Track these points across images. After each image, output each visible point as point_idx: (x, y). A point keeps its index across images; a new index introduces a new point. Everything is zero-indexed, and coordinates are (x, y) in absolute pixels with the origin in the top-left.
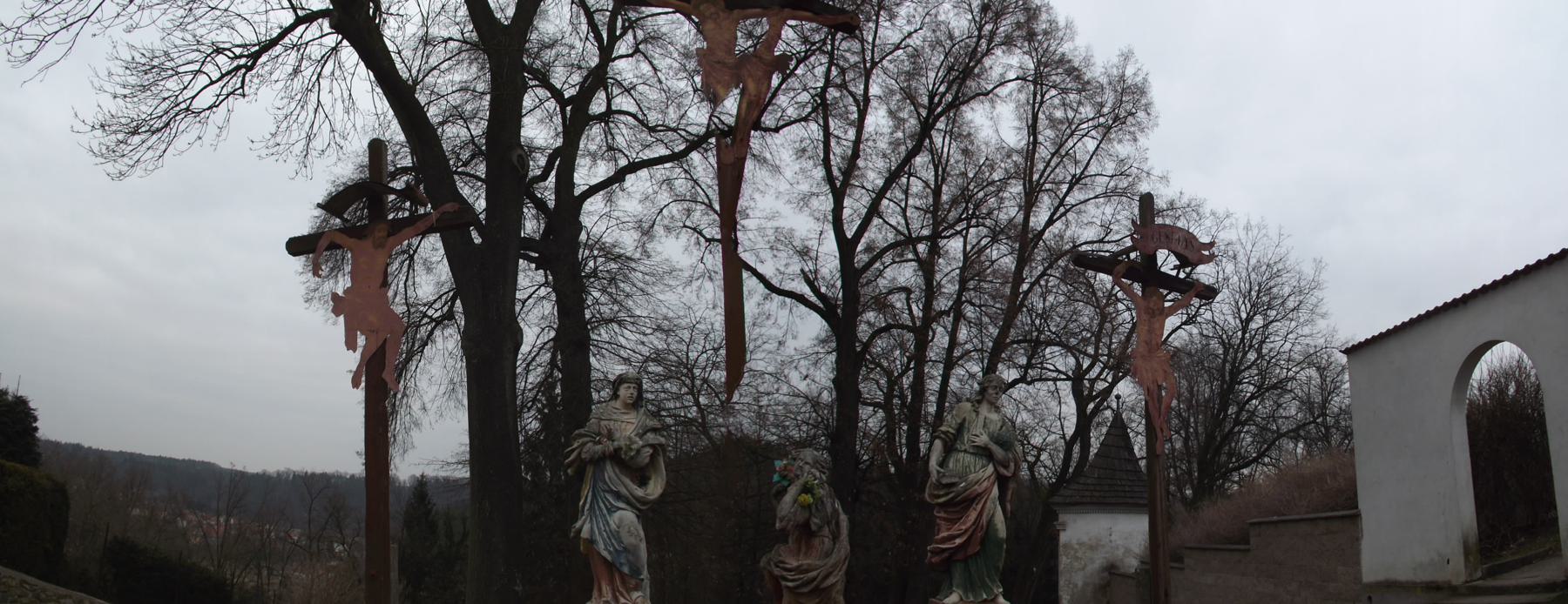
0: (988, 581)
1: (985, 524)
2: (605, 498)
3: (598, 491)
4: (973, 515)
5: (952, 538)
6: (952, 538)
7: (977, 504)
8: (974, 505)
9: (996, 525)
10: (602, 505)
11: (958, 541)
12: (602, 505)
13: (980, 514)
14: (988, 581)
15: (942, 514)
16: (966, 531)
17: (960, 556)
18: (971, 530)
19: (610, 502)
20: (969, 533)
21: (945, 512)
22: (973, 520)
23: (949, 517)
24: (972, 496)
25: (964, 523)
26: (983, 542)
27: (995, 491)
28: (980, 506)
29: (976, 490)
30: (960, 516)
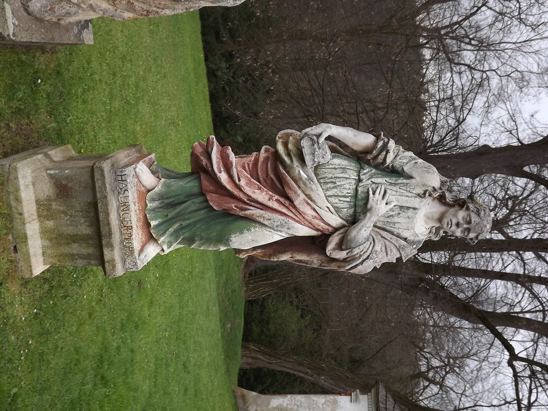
0: (176, 226)
1: (248, 212)
4: (262, 196)
5: (228, 168)
6: (228, 168)
7: (277, 201)
8: (277, 197)
9: (248, 230)
11: (223, 177)
14: (176, 226)
15: (263, 154)
16: (239, 187)
17: (206, 183)
18: (241, 195)
20: (236, 192)
21: (267, 159)
22: (254, 196)
23: (260, 164)
24: (288, 191)
25: (249, 184)
26: (227, 214)
27: (303, 231)
28: (276, 205)
29: (298, 196)
30: (261, 179)
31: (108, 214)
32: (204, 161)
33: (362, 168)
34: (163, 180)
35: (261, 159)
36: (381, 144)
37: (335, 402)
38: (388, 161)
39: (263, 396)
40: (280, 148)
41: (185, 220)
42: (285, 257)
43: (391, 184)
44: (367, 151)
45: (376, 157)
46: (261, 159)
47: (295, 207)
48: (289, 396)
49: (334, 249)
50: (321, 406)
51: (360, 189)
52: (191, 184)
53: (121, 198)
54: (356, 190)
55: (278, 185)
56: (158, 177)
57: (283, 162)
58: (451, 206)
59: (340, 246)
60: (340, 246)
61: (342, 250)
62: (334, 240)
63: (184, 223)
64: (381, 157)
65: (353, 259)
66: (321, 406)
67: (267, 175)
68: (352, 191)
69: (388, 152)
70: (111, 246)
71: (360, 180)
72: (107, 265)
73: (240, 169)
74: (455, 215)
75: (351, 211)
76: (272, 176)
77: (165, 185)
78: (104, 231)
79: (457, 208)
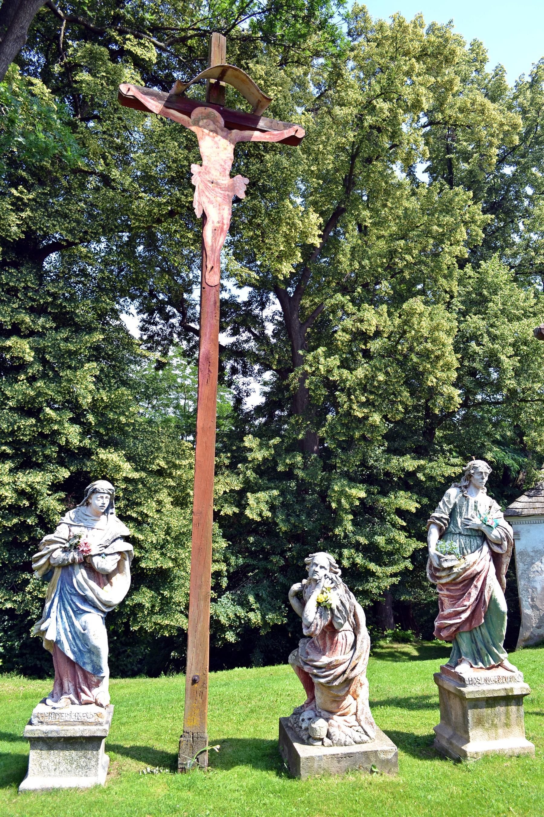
2: (72, 600)
3: (65, 594)
4: (474, 593)
5: (458, 614)
7: (477, 582)
8: (475, 582)
10: (69, 608)
11: (464, 616)
12: (69, 608)
13: (482, 591)
17: (466, 628)
18: (474, 605)
19: (77, 606)
21: (448, 590)
24: (472, 576)
28: (479, 585)
31: (494, 690)
32: (454, 629)
33: (451, 532)
34: (463, 657)
35: (448, 593)
36: (438, 522)
37: (521, 553)
38: (447, 517)
39: (523, 621)
40: (444, 581)
41: (488, 642)
42: (505, 580)
43: (461, 516)
44: (440, 529)
45: (445, 524)
46: (448, 593)
47: (480, 572)
48: (520, 596)
49: (501, 548)
50: (526, 566)
51: (465, 533)
52: (465, 639)
53: (482, 681)
54: (466, 535)
55: (466, 582)
56: (461, 661)
57: (454, 579)
58: (470, 481)
59: (499, 545)
60: (499, 545)
61: (502, 544)
62: (496, 549)
63: (491, 643)
64: (446, 522)
65: (507, 537)
66: (526, 566)
67: (459, 589)
68: (467, 538)
69: (442, 517)
70: (512, 690)
71: (460, 534)
72: (524, 693)
73: (456, 606)
74: (477, 480)
75: (478, 538)
76: (461, 586)
77: (466, 655)
78: (503, 694)
79: (472, 479)
